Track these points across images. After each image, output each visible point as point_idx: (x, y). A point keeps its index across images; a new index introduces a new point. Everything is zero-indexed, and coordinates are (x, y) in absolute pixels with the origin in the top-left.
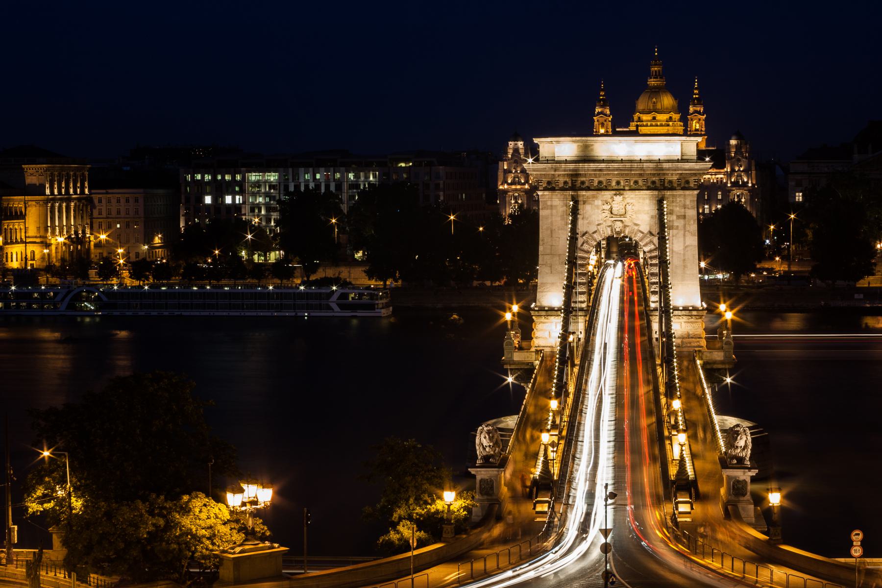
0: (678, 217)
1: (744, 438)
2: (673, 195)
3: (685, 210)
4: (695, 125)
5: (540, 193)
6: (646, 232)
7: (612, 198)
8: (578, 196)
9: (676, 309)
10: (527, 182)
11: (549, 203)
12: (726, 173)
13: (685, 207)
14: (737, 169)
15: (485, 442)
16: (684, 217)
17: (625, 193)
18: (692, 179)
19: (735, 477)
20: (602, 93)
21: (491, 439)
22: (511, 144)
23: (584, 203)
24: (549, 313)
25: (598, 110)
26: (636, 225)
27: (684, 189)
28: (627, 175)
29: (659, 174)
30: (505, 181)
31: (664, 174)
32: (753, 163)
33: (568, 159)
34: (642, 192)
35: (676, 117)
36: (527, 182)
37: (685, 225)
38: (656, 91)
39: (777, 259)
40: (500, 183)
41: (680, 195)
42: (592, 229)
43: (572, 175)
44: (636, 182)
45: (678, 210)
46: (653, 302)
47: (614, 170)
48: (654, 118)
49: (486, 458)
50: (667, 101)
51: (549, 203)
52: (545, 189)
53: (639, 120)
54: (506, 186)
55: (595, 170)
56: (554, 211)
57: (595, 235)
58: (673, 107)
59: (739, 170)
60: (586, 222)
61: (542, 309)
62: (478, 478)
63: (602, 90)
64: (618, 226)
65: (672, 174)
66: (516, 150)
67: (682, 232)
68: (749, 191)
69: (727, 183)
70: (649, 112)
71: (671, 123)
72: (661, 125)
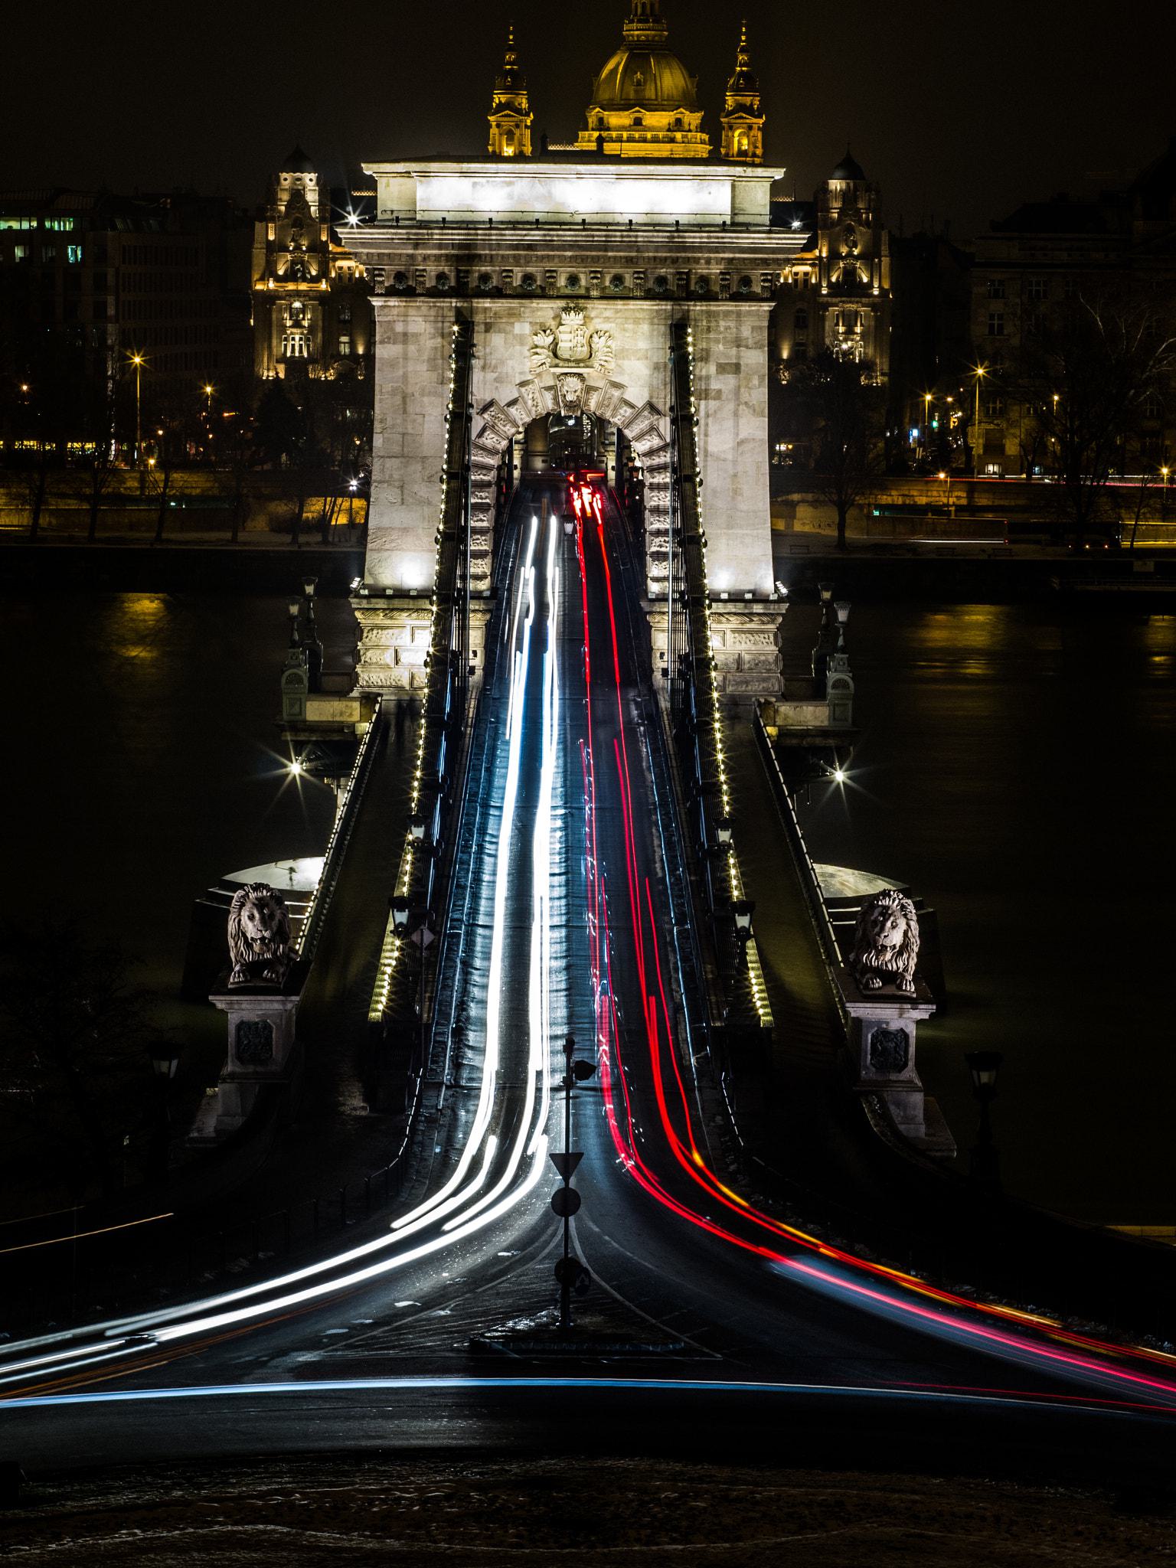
0: (722, 369)
1: (902, 924)
2: (710, 314)
3: (738, 347)
4: (739, 140)
5: (376, 302)
6: (640, 404)
7: (557, 317)
8: (472, 311)
9: (715, 598)
10: (324, 273)
11: (399, 328)
12: (818, 262)
13: (738, 343)
14: (844, 250)
15: (251, 929)
16: (737, 368)
17: (590, 304)
18: (757, 274)
19: (879, 1023)
20: (510, 57)
21: (265, 922)
22: (287, 179)
23: (488, 328)
24: (397, 603)
25: (499, 98)
26: (616, 385)
27: (736, 297)
29: (675, 261)
30: (270, 272)
32: (885, 237)
33: (449, 217)
34: (633, 305)
35: (693, 119)
36: (324, 273)
37: (737, 391)
38: (640, 56)
39: (942, 476)
40: (256, 277)
41: (727, 314)
42: (505, 395)
44: (618, 279)
45: (720, 350)
46: (656, 580)
48: (638, 122)
49: (253, 969)
50: (671, 80)
51: (399, 328)
52: (391, 292)
53: (602, 125)
54: (272, 285)
55: (516, 247)
56: (412, 348)
57: (513, 410)
58: (685, 94)
59: (850, 255)
60: (491, 376)
61: (377, 593)
62: (233, 1019)
63: (511, 49)
64: (572, 388)
65: (708, 261)
66: (298, 195)
67: (731, 406)
68: (874, 307)
69: (819, 285)
70: (626, 107)
71: (678, 135)
72: (655, 140)
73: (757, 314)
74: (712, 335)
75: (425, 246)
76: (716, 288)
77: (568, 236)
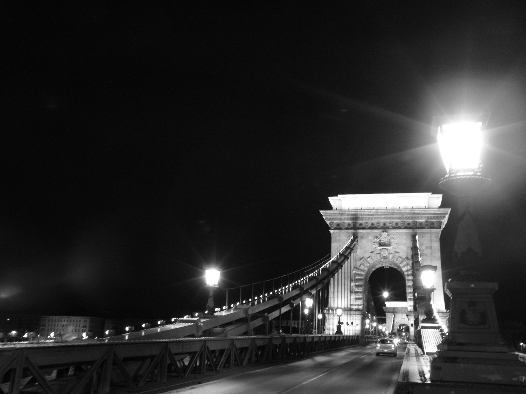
0: (427, 248)
2: (423, 233)
5: (331, 231)
6: (404, 257)
8: (357, 233)
16: (431, 247)
23: (362, 238)
28: (390, 218)
29: (412, 218)
31: (415, 217)
37: (432, 253)
41: (428, 233)
42: (367, 255)
43: (353, 219)
47: (381, 215)
51: (338, 238)
52: (335, 229)
57: (369, 259)
60: (362, 251)
64: (385, 253)
73: (436, 233)
74: (424, 239)
75: (344, 215)
76: (423, 225)
77: (383, 211)
